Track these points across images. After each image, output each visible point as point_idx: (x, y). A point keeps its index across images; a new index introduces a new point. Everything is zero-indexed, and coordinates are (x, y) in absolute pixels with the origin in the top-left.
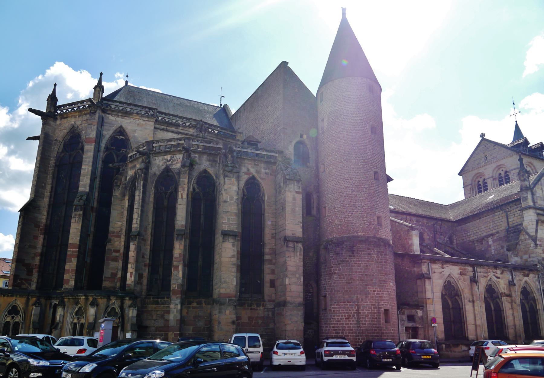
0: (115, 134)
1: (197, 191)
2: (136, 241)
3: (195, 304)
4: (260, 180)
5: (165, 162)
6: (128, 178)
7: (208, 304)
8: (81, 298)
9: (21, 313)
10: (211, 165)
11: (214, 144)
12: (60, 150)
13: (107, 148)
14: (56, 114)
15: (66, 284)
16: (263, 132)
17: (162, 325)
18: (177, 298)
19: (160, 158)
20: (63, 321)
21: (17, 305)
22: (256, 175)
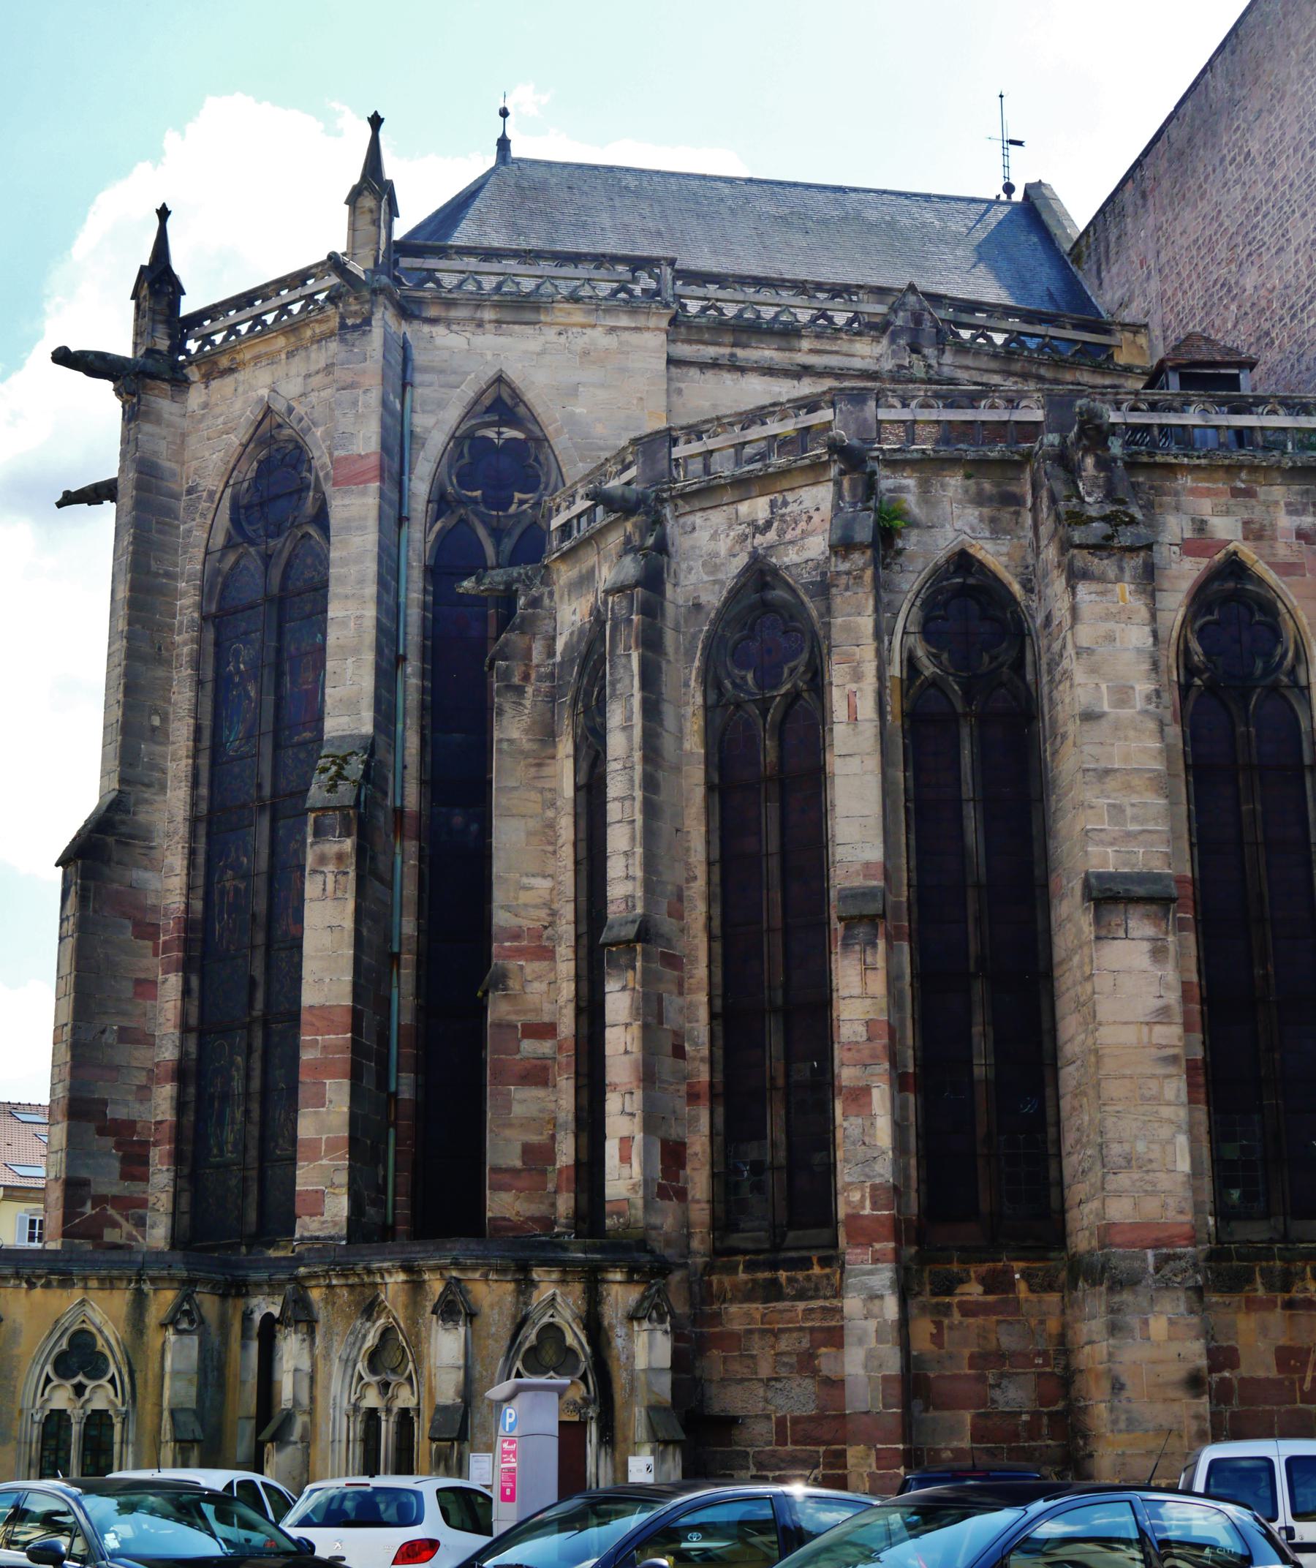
0: (473, 422)
1: (927, 673)
2: (634, 968)
3: (973, 1291)
4: (1271, 577)
5: (744, 537)
6: (560, 645)
7: (1050, 1288)
8: (388, 1279)
9: (113, 1369)
10: (993, 520)
11: (993, 407)
12: (219, 540)
13: (441, 502)
14: (182, 358)
15: (311, 1215)
16: (1263, 303)
17: (810, 1410)
18: (876, 1261)
19: (718, 518)
20: (312, 1399)
21: (94, 1331)
22: (1248, 552)
